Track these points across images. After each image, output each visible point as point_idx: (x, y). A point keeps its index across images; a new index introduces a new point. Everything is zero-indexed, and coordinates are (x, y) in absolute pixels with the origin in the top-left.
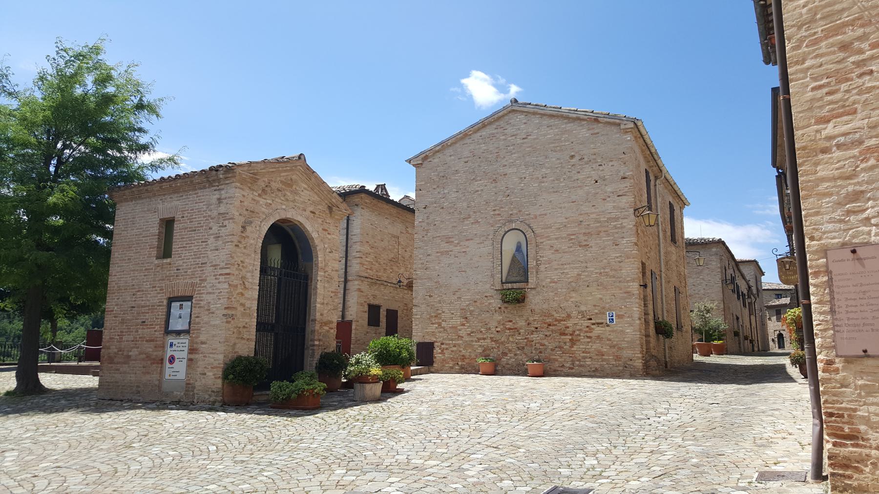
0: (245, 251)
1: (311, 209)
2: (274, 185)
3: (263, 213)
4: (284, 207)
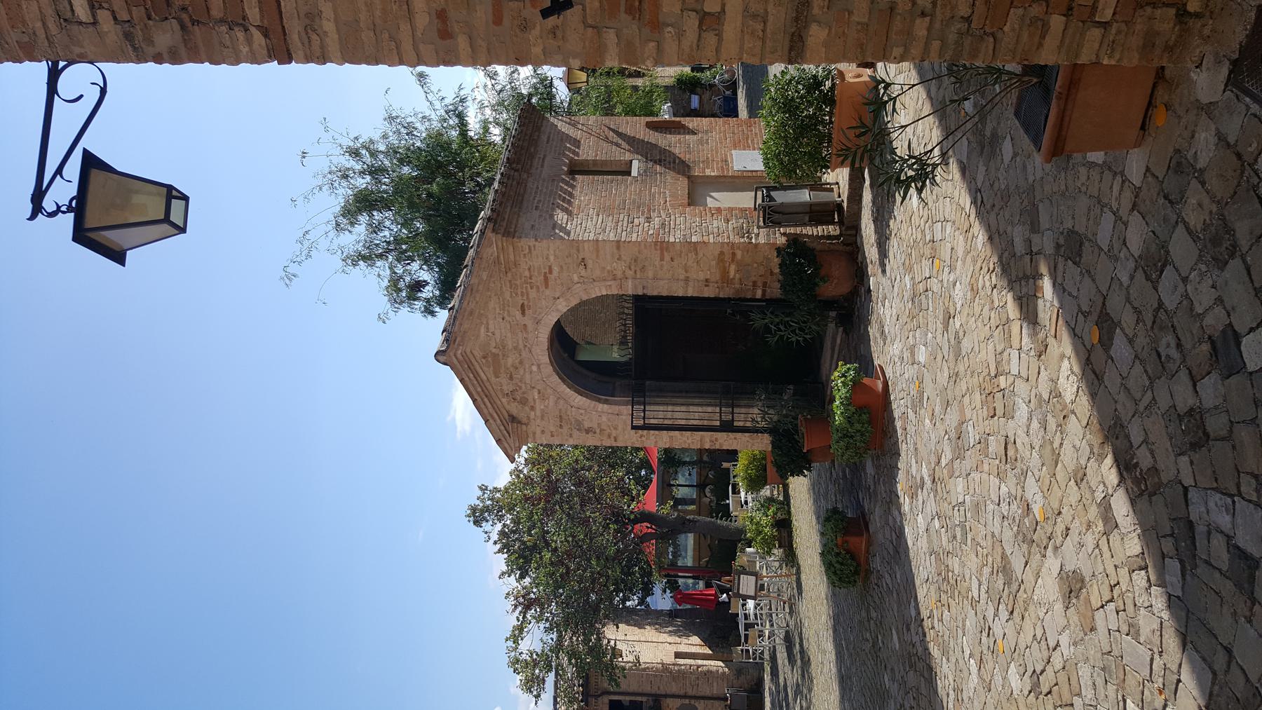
0: (620, 428)
1: (518, 314)
2: (507, 388)
3: (556, 402)
4: (534, 368)
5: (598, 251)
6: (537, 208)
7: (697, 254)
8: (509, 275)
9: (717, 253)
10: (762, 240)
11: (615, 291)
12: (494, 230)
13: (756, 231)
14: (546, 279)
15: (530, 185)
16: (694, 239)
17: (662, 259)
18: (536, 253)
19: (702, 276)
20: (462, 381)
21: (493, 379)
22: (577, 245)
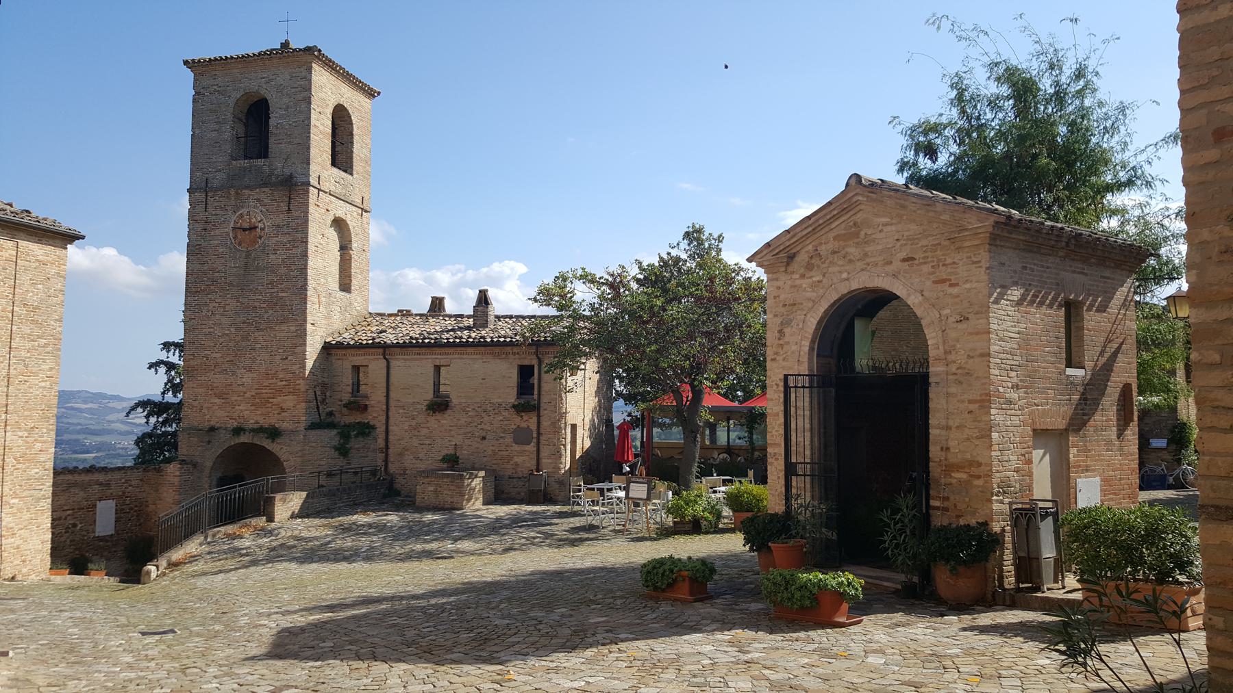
0: (785, 364)
1: (903, 255)
2: (823, 250)
3: (809, 299)
4: (845, 275)
5: (977, 334)
6: (1025, 268)
7: (977, 438)
8: (947, 243)
9: (980, 459)
10: (996, 506)
11: (932, 353)
12: (997, 223)
13: (1007, 500)
14: (944, 281)
15: (1051, 259)
16: (995, 435)
17: (970, 402)
18: (972, 270)
19: (952, 444)
20: (830, 203)
21: (831, 235)
22: (984, 311)
